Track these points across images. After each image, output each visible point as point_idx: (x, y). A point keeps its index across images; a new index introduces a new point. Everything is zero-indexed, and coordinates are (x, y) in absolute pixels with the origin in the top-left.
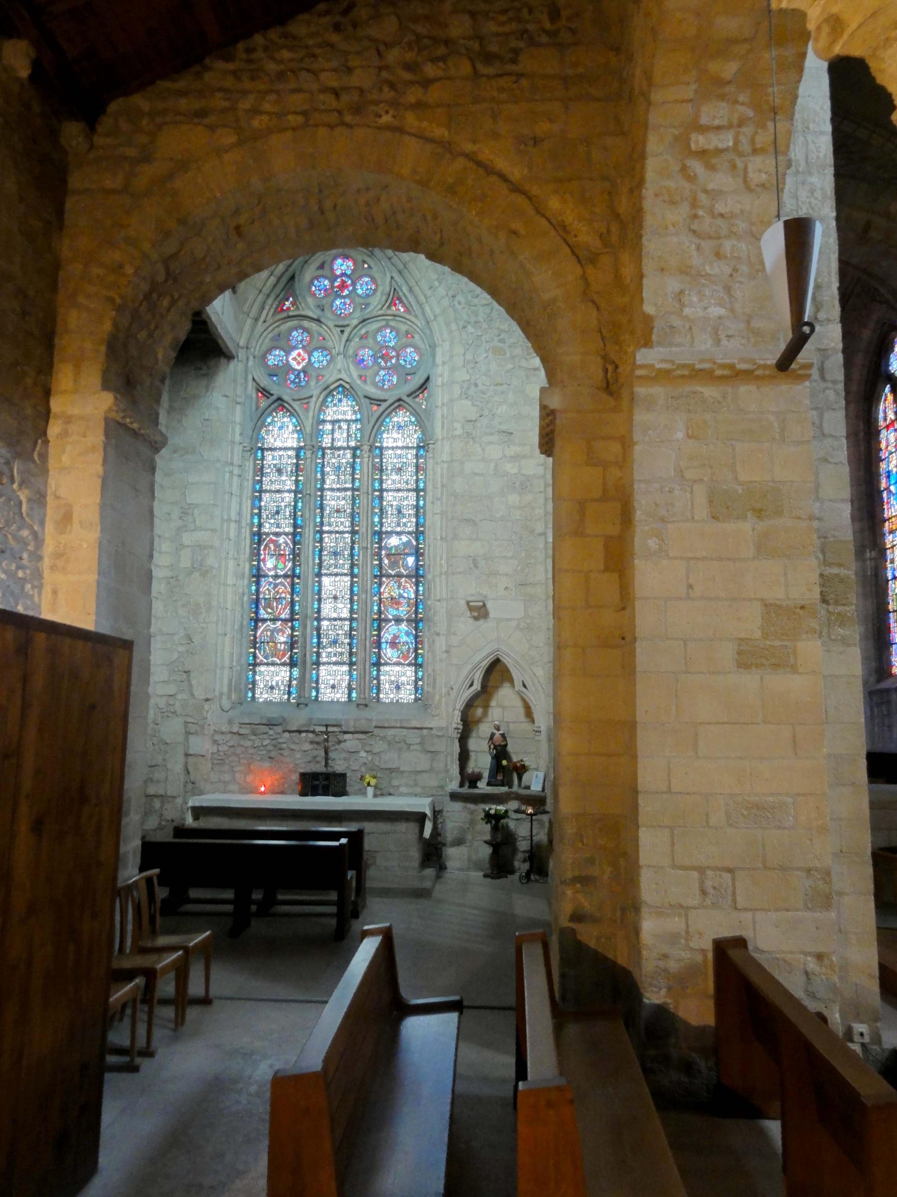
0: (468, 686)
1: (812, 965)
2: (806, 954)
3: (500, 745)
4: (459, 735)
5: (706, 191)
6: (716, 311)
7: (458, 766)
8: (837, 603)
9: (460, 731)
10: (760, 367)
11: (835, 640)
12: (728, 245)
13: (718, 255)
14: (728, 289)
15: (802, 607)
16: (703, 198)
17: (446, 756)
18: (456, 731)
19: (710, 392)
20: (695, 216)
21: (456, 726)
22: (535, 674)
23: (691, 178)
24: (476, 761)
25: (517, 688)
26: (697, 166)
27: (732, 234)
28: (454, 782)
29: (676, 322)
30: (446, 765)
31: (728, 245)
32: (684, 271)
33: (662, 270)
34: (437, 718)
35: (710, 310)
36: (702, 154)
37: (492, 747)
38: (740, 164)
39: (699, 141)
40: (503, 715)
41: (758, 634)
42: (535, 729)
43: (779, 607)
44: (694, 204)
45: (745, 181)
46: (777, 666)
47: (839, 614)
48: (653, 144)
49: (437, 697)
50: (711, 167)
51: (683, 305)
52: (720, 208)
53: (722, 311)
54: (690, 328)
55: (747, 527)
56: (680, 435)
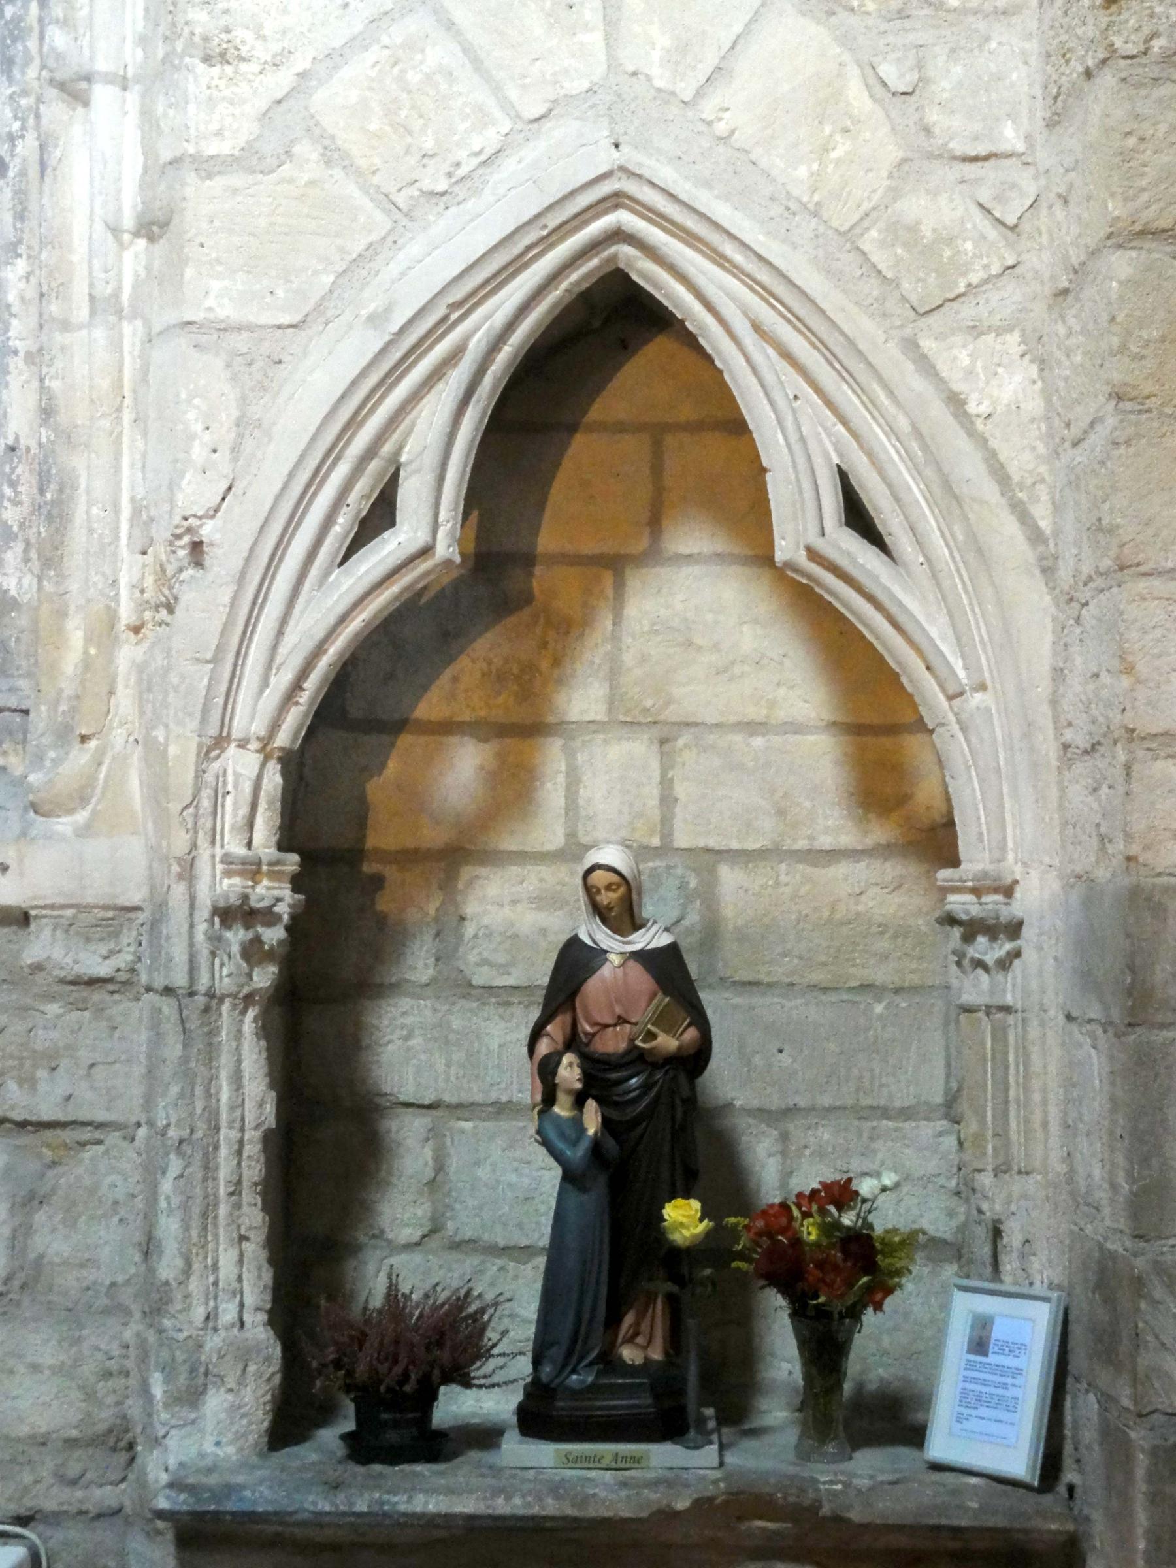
0: (344, 524)
3: (636, 1058)
4: (265, 977)
7: (255, 1250)
9: (273, 935)
17: (152, 1172)
18: (236, 937)
21: (231, 887)
22: (956, 402)
24: (434, 1185)
25: (785, 549)
28: (215, 1402)
30: (149, 1248)
34: (64, 825)
37: (569, 1072)
40: (667, 800)
42: (962, 904)
49: (76, 637)
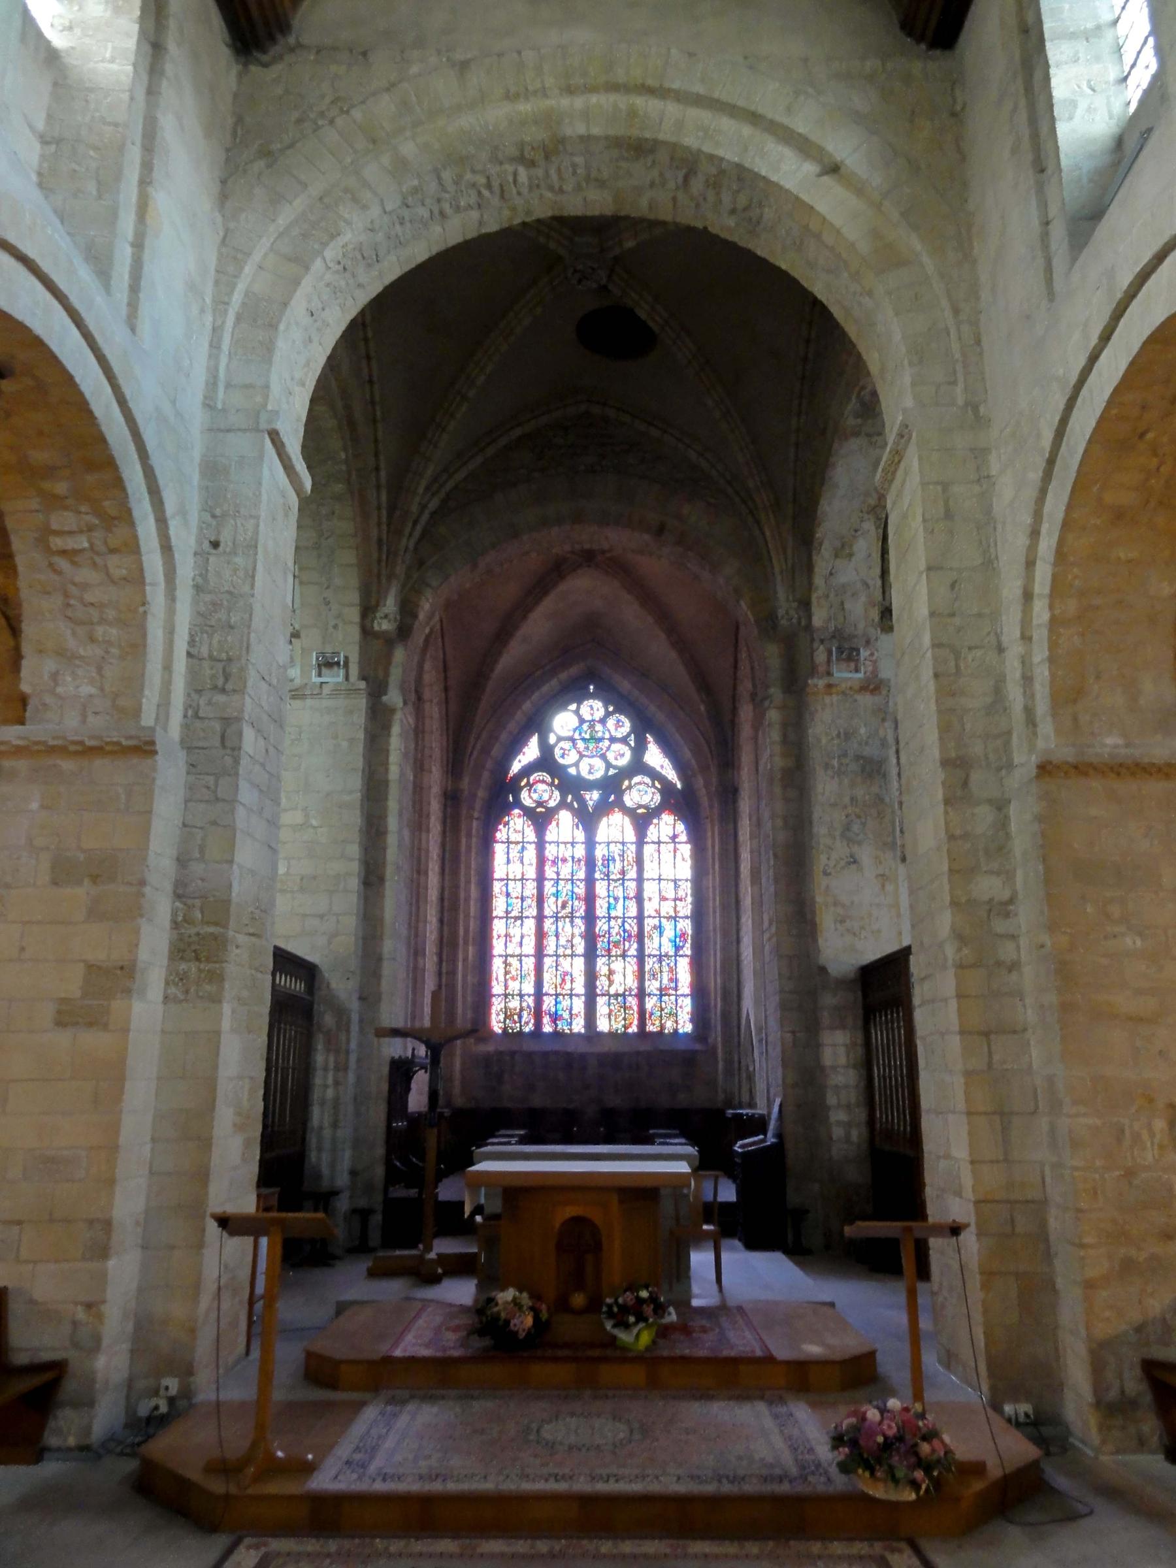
1: (81, 1314)
2: (76, 1304)
5: (75, 584)
6: (87, 690)
8: (208, 960)
10: (107, 743)
11: (202, 997)
12: (100, 631)
13: (92, 639)
14: (100, 669)
15: (122, 968)
16: (73, 590)
19: (67, 765)
20: (68, 605)
23: (59, 572)
26: (63, 564)
27: (102, 621)
29: (48, 699)
31: (100, 631)
32: (61, 653)
33: (41, 651)
35: (80, 689)
36: (63, 553)
38: (98, 559)
39: (57, 542)
41: (78, 994)
43: (99, 968)
44: (66, 595)
45: (108, 574)
46: (90, 1024)
47: (209, 971)
48: (17, 544)
50: (74, 563)
51: (57, 684)
52: (89, 597)
53: (93, 691)
54: (61, 706)
55: (82, 892)
56: (34, 806)
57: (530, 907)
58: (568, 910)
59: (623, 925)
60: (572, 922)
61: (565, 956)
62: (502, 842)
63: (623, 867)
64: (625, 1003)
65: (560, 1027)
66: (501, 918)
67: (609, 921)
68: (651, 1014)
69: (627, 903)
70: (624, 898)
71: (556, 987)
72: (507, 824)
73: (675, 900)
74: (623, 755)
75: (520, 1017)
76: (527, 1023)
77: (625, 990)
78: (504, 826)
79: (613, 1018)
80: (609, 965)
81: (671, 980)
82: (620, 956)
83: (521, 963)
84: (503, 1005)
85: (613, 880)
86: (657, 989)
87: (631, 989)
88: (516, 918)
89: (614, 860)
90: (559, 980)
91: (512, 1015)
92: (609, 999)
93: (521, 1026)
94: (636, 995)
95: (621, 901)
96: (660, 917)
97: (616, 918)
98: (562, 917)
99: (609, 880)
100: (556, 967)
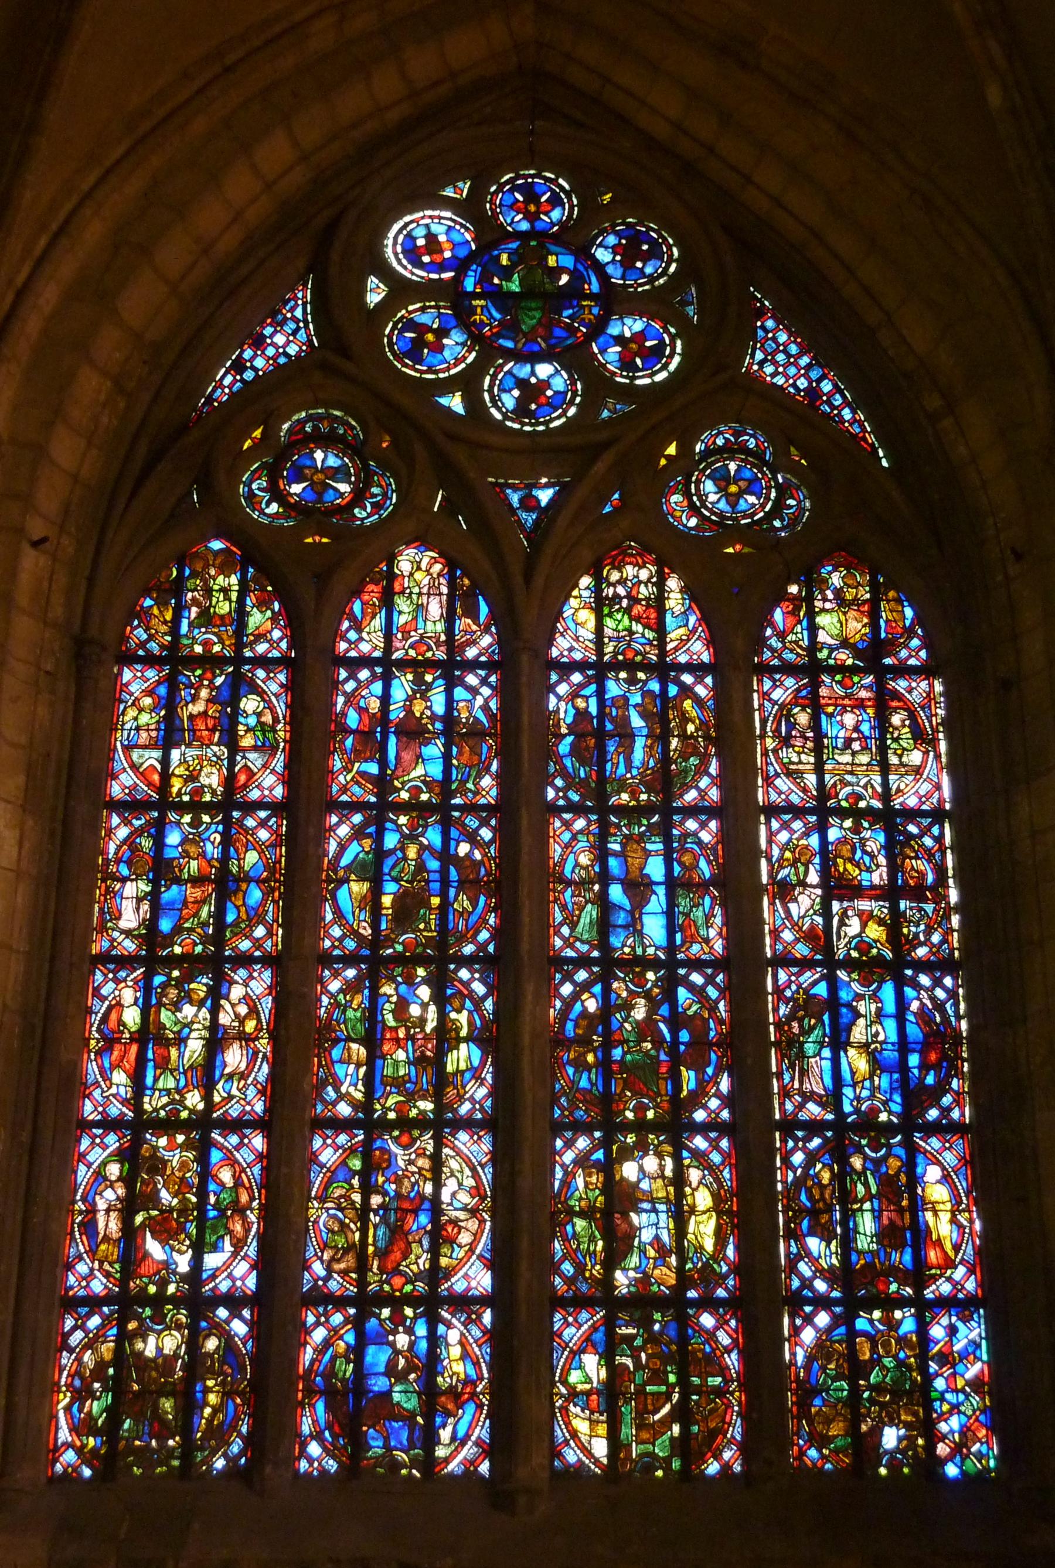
57: (256, 916)
58: (428, 927)
59: (670, 997)
60: (440, 983)
61: (405, 1124)
62: (150, 660)
63: (665, 760)
64: (683, 1340)
65: (376, 1446)
66: (126, 962)
67: (606, 979)
68: (808, 1391)
69: (683, 904)
70: (671, 883)
71: (362, 1267)
72: (178, 588)
73: (890, 893)
74: (656, 354)
75: (189, 1405)
76: (219, 1435)
77: (684, 1280)
78: (162, 603)
79: (628, 1411)
80: (608, 1167)
81: (888, 1236)
82: (655, 1127)
83: (203, 1159)
84: (107, 1349)
85: (621, 810)
86: (829, 1275)
87: (708, 1277)
88: (191, 964)
89: (627, 736)
90: (377, 1234)
91: (151, 1394)
92: (610, 1323)
93: (188, 1448)
94: (734, 1304)
95: (657, 901)
96: (831, 964)
97: (638, 964)
98: (398, 959)
99: (603, 810)
100: (366, 1174)
